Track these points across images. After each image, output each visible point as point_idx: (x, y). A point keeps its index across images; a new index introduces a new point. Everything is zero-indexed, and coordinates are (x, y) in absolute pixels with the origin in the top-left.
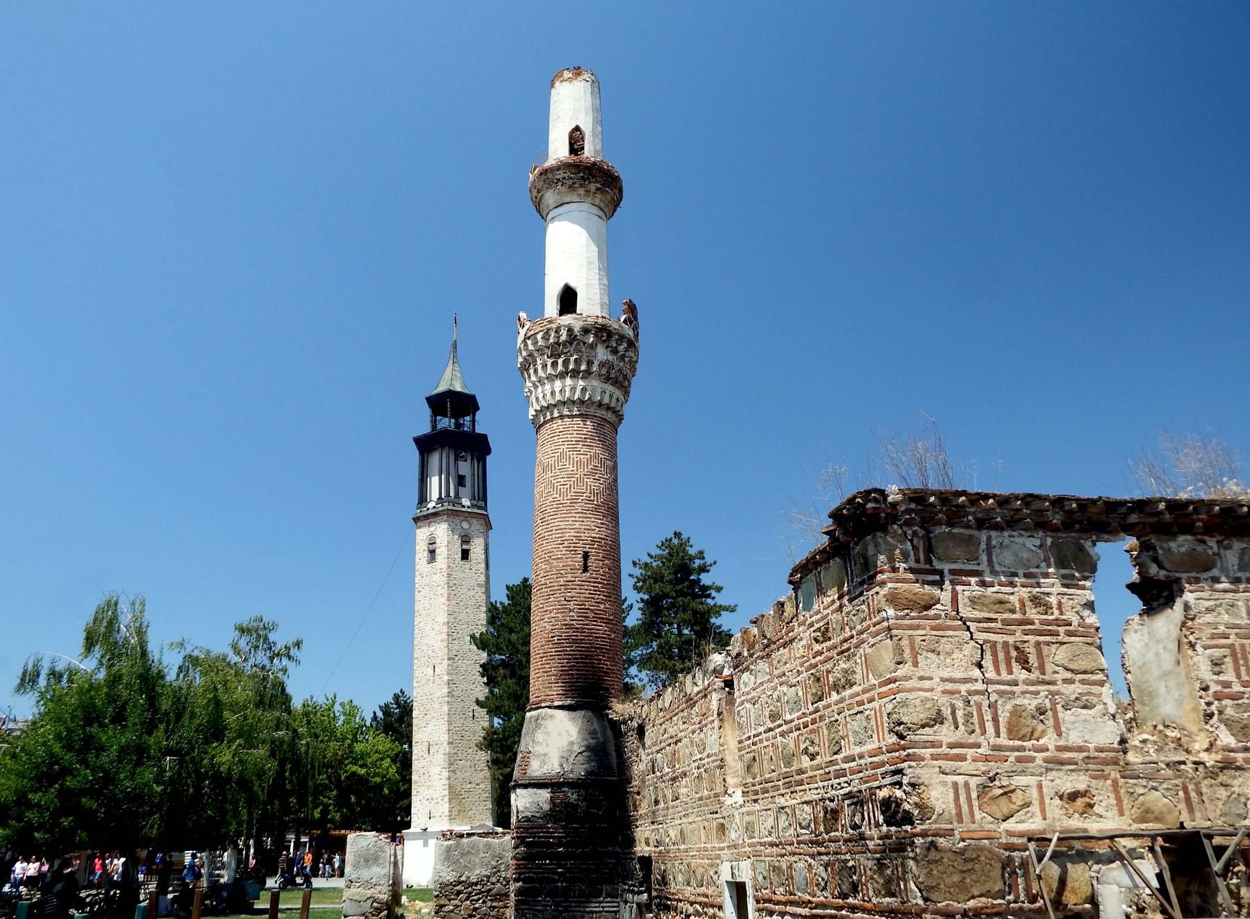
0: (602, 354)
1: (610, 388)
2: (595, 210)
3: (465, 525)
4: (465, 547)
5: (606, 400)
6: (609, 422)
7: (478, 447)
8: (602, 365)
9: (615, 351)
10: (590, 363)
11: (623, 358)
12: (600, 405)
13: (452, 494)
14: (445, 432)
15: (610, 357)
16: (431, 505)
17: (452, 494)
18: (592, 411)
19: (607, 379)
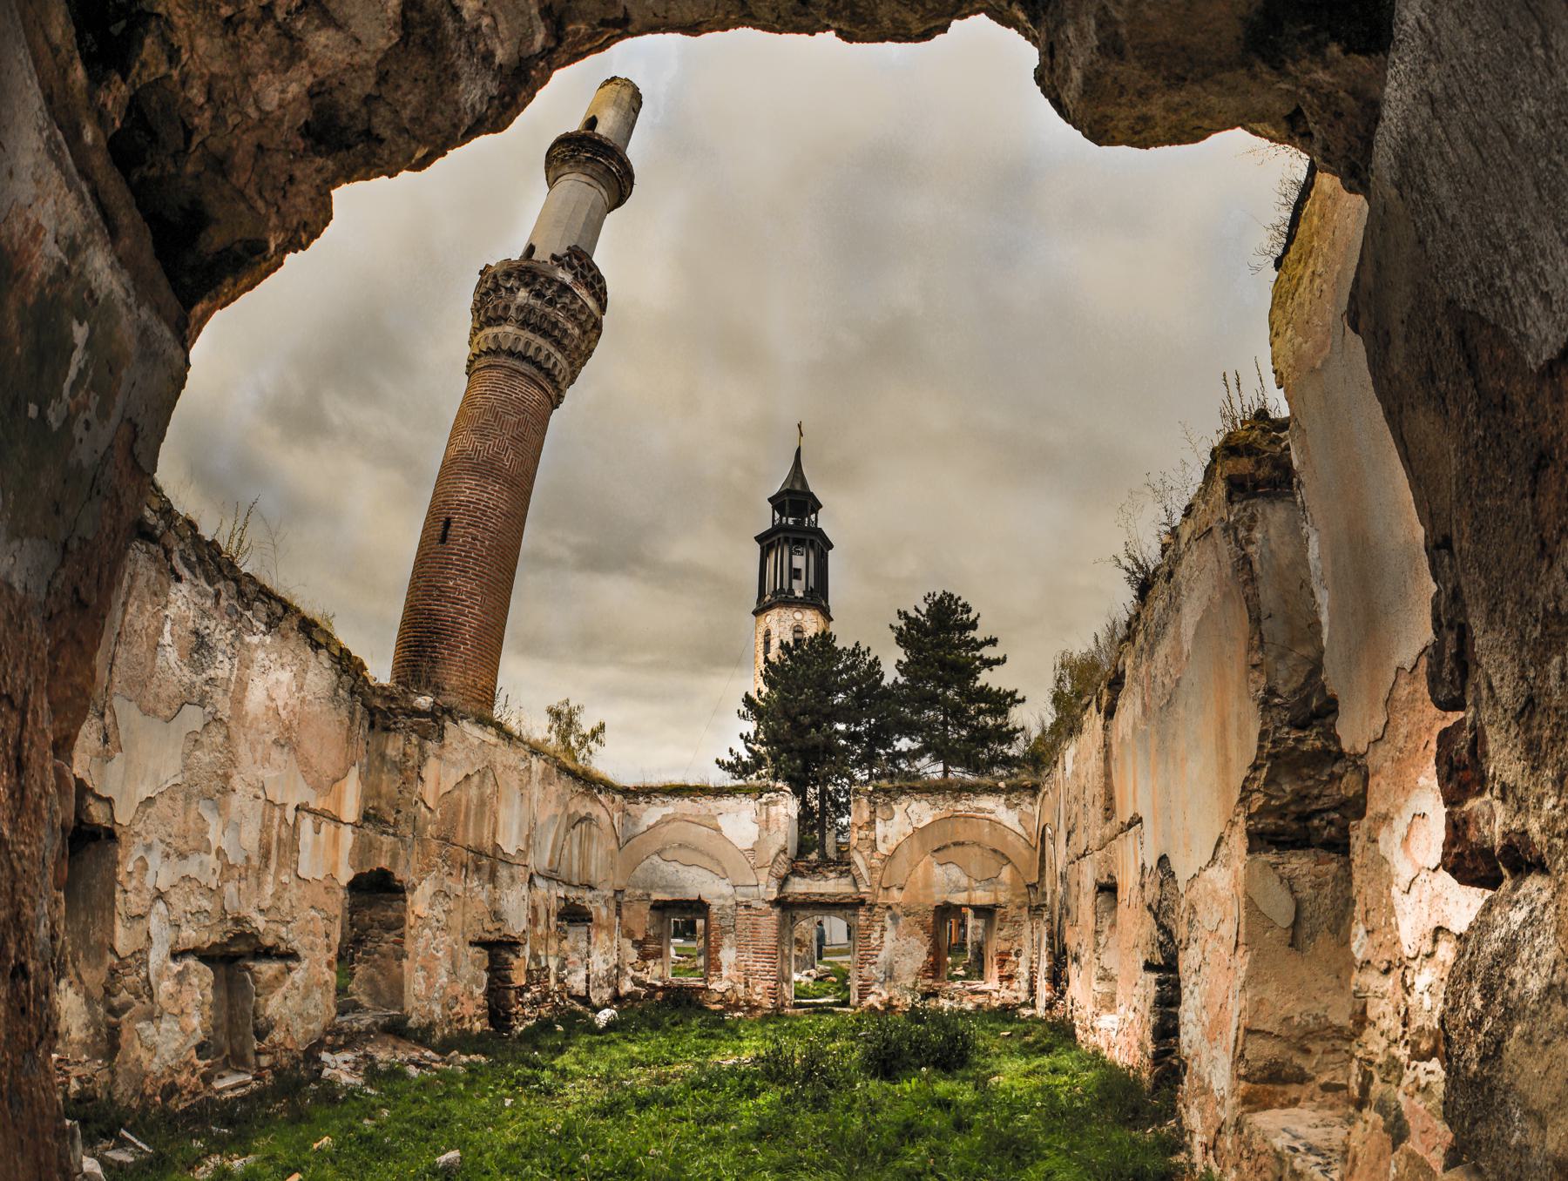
0: (522, 295)
1: (527, 335)
2: (584, 178)
3: (798, 616)
4: (798, 636)
5: (520, 347)
6: (523, 375)
7: (819, 545)
8: (520, 309)
9: (539, 295)
10: (507, 308)
11: (551, 302)
12: (511, 353)
13: (786, 587)
14: (786, 528)
15: (532, 302)
16: (768, 598)
17: (786, 587)
18: (502, 360)
19: (524, 324)
